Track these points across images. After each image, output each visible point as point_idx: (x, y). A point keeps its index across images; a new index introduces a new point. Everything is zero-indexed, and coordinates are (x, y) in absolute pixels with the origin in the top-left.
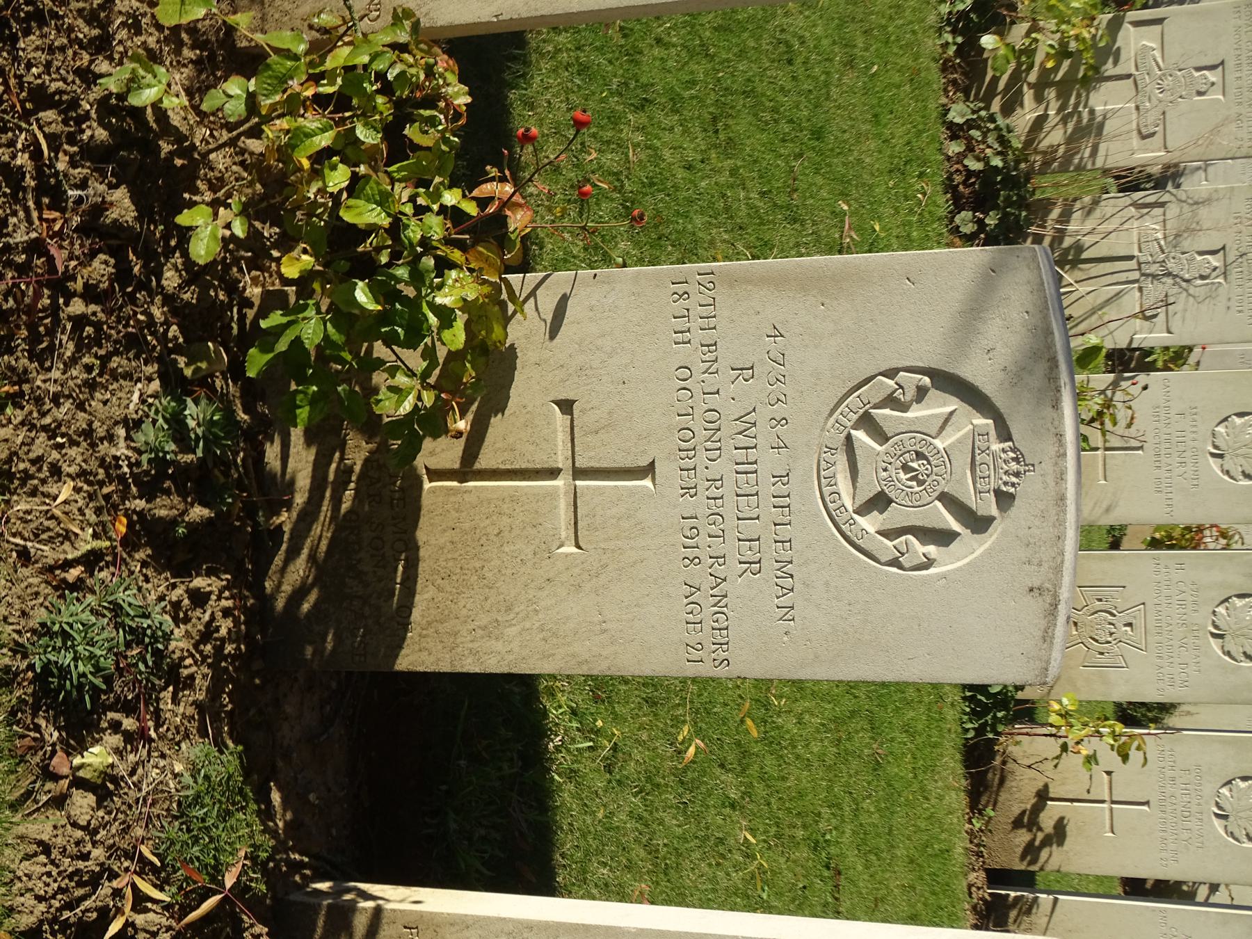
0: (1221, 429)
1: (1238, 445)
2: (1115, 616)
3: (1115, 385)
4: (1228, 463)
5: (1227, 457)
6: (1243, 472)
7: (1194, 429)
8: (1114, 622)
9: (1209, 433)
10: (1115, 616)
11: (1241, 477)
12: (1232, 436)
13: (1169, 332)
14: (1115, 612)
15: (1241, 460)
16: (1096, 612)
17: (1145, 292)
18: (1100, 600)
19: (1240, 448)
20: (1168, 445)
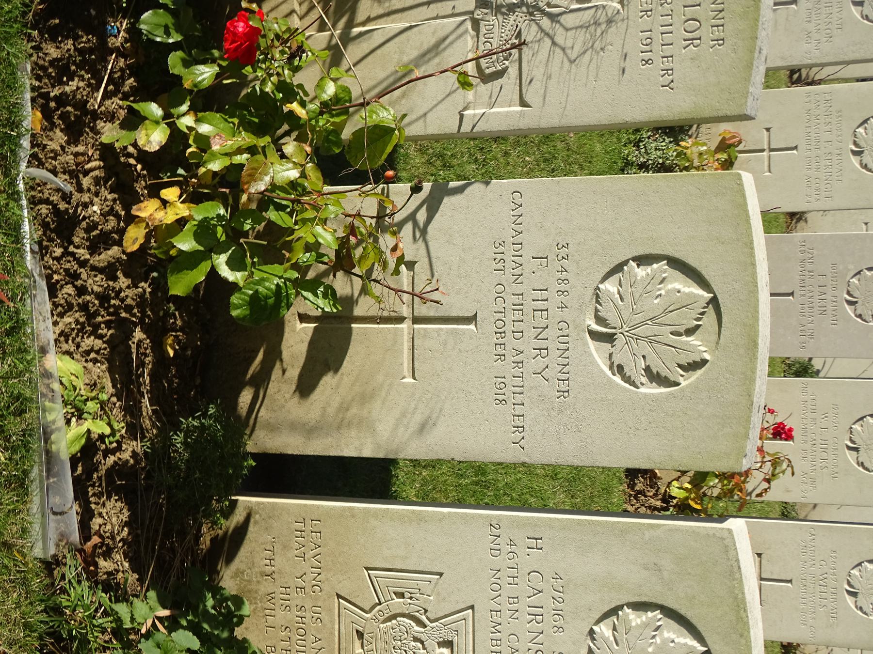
0: (610, 287)
2: (425, 626)
3: (433, 205)
5: (620, 340)
6: (648, 369)
7: (563, 287)
8: (423, 637)
9: (591, 291)
10: (425, 626)
11: (644, 380)
12: (628, 298)
13: (523, 103)
14: (423, 618)
15: (644, 347)
16: (394, 617)
17: (483, 30)
18: (401, 595)
19: (643, 323)
20: (518, 316)
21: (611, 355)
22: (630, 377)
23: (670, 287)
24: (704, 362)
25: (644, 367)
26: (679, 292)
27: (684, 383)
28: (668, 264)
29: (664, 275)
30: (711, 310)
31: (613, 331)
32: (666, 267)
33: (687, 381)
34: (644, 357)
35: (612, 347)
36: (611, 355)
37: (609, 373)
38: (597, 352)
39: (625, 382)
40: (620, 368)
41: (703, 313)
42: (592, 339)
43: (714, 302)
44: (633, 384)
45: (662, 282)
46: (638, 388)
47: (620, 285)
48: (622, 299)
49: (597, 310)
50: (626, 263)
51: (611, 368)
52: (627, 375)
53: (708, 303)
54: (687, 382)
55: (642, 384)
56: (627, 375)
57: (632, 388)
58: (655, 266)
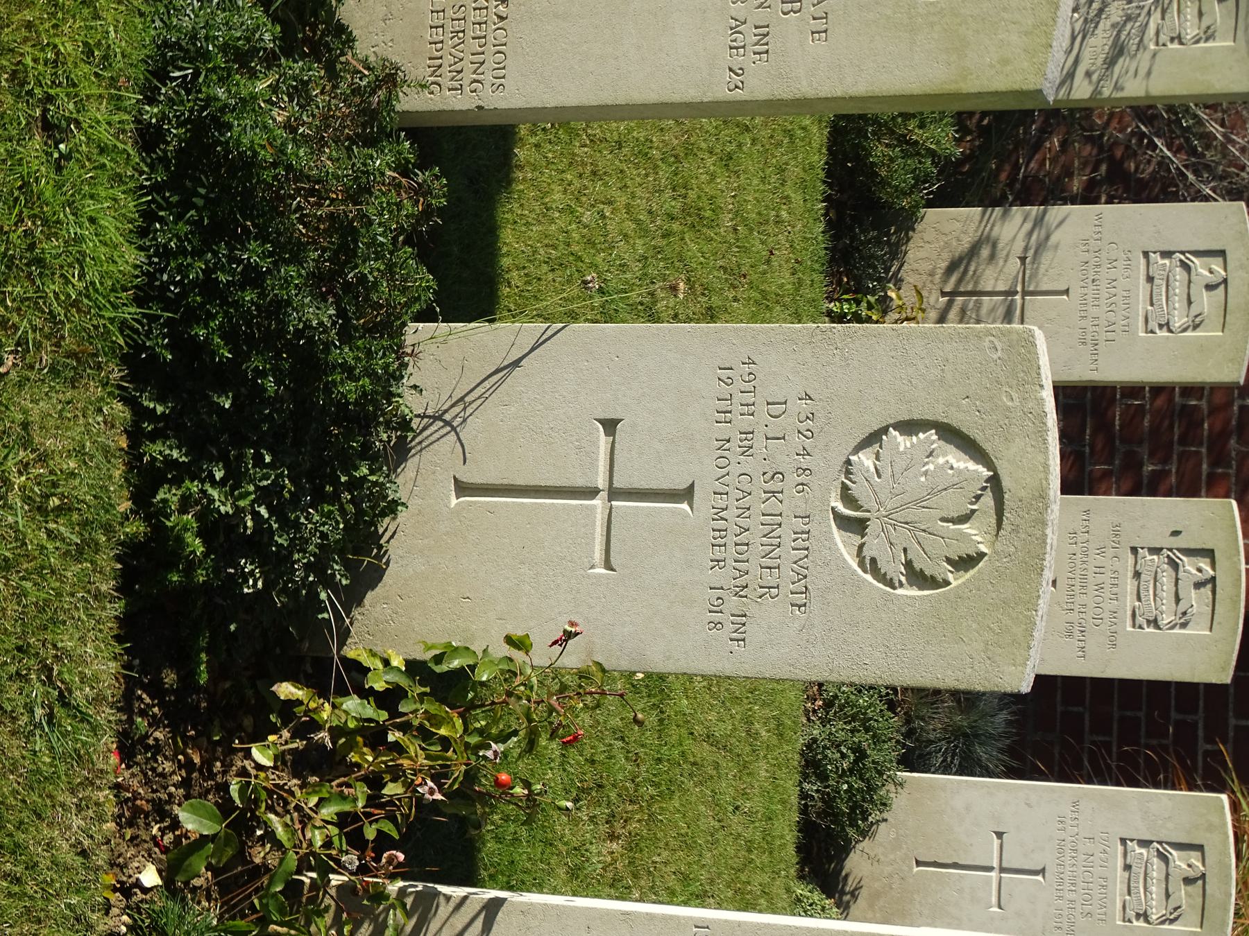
0: (865, 459)
1: (895, 502)
4: (875, 545)
5: (873, 527)
6: (909, 564)
11: (903, 579)
15: (902, 536)
21: (861, 547)
22: (885, 574)
23: (941, 460)
24: (982, 555)
25: (903, 561)
26: (952, 468)
27: (954, 584)
28: (936, 434)
29: (933, 447)
30: (989, 493)
31: (867, 515)
32: (935, 437)
33: (956, 580)
34: (905, 550)
35: (863, 537)
36: (861, 547)
37: (859, 571)
38: (843, 543)
39: (879, 582)
40: (873, 561)
41: (978, 497)
42: (839, 527)
43: (995, 482)
44: (891, 584)
45: (931, 454)
46: (894, 588)
47: (878, 458)
48: (879, 476)
49: (845, 488)
50: (885, 430)
51: (861, 564)
52: (883, 571)
53: (986, 481)
54: (960, 581)
55: (901, 585)
56: (883, 571)
57: (888, 589)
58: (921, 435)
